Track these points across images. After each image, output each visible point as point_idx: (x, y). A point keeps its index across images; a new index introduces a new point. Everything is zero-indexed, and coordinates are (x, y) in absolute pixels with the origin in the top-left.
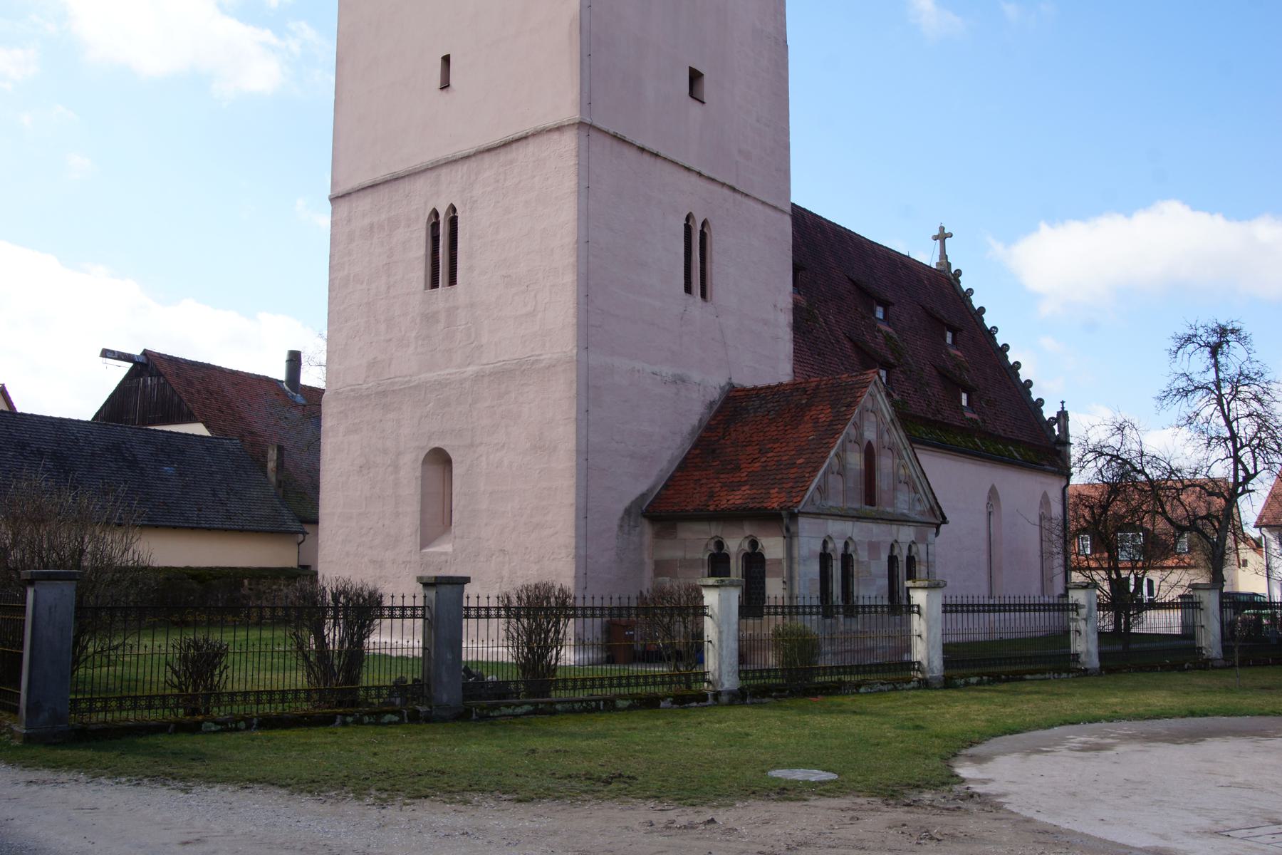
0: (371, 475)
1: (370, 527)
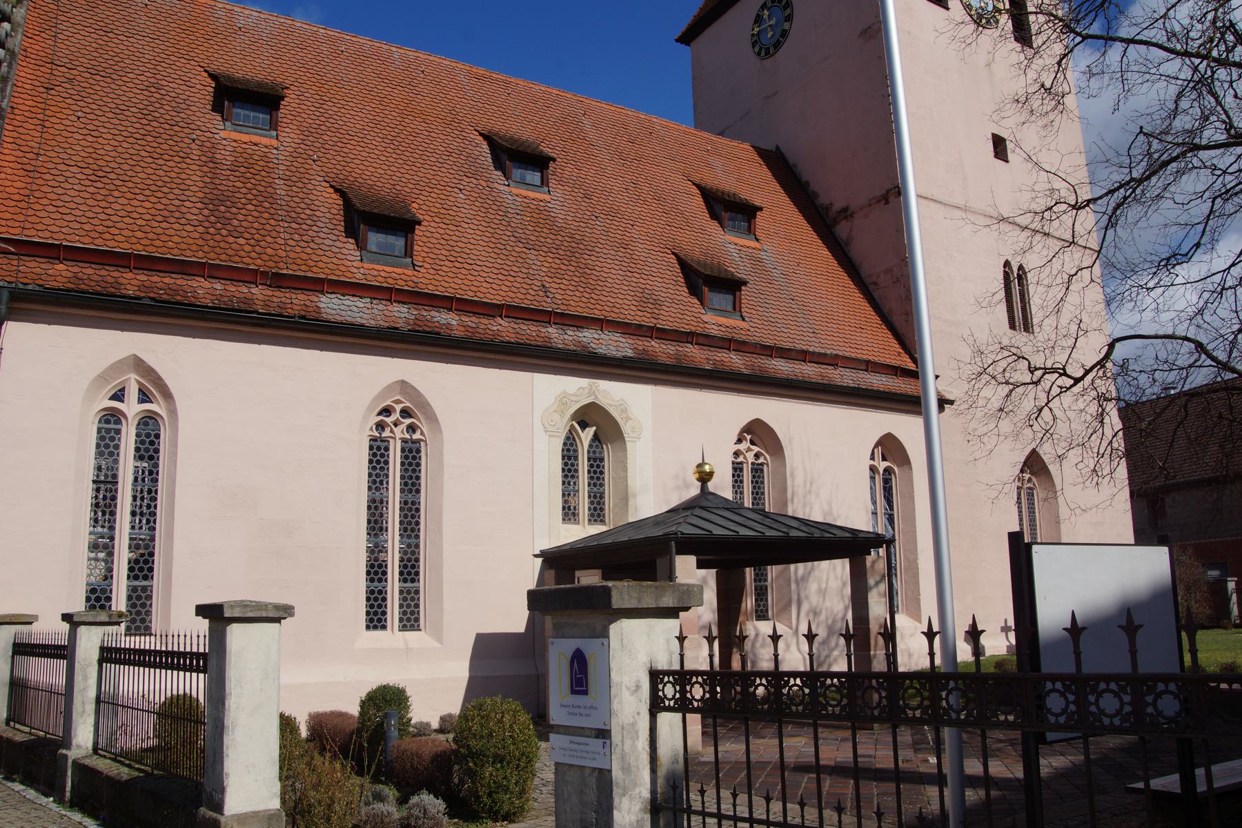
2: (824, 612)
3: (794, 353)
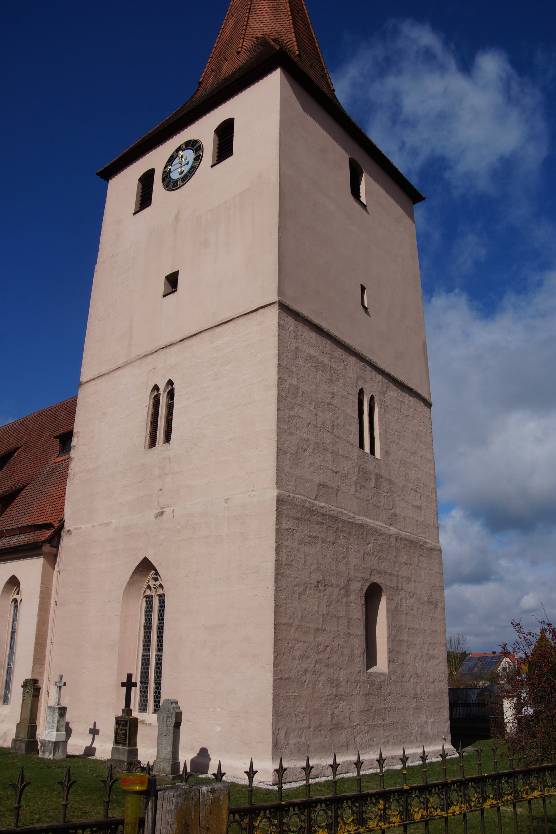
0: (327, 592)
1: (326, 644)
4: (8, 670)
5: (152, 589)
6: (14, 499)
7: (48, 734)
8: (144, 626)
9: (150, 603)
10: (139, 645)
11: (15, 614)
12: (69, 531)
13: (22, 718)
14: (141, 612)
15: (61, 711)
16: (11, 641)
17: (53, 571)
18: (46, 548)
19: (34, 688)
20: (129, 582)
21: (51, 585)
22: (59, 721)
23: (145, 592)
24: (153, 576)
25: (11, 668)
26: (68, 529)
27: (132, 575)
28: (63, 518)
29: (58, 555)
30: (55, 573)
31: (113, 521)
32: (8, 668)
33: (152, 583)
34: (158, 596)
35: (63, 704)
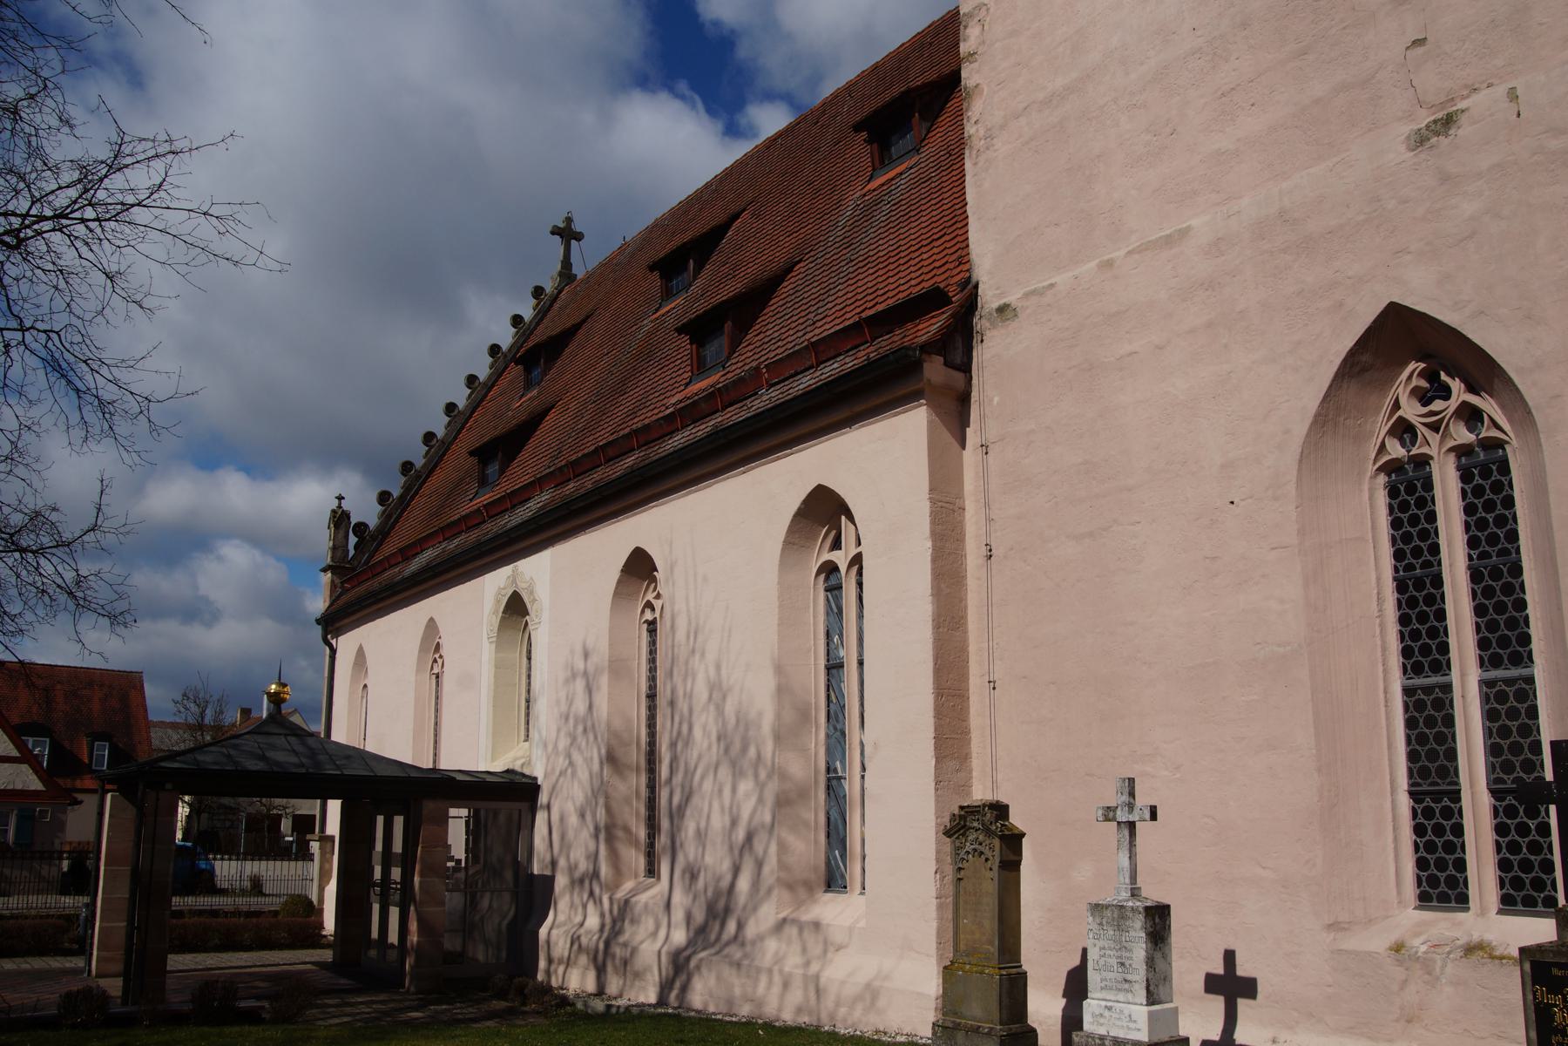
2: (702, 874)
3: (703, 405)
4: (829, 787)
5: (1421, 430)
6: (764, 304)
7: (1107, 1013)
8: (1395, 579)
9: (1411, 490)
10: (1384, 649)
11: (835, 612)
12: (1002, 309)
13: (962, 947)
14: (1374, 527)
15: (1154, 920)
16: (828, 696)
17: (956, 446)
18: (934, 370)
19: (1002, 838)
20: (1317, 415)
21: (960, 496)
22: (1153, 958)
23: (1382, 448)
24: (1415, 382)
25: (840, 778)
26: (995, 305)
27: (1330, 386)
28: (970, 277)
29: (974, 395)
30: (970, 456)
31: (1194, 222)
32: (829, 780)
33: (1411, 411)
34: (1452, 455)
35: (1154, 893)
